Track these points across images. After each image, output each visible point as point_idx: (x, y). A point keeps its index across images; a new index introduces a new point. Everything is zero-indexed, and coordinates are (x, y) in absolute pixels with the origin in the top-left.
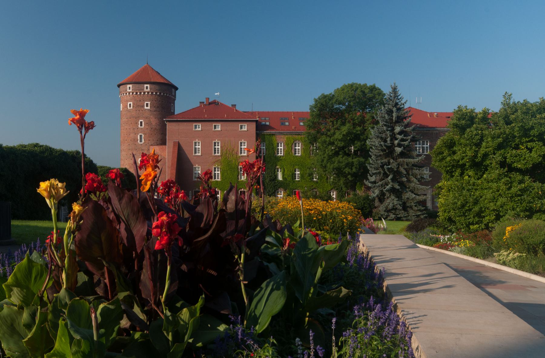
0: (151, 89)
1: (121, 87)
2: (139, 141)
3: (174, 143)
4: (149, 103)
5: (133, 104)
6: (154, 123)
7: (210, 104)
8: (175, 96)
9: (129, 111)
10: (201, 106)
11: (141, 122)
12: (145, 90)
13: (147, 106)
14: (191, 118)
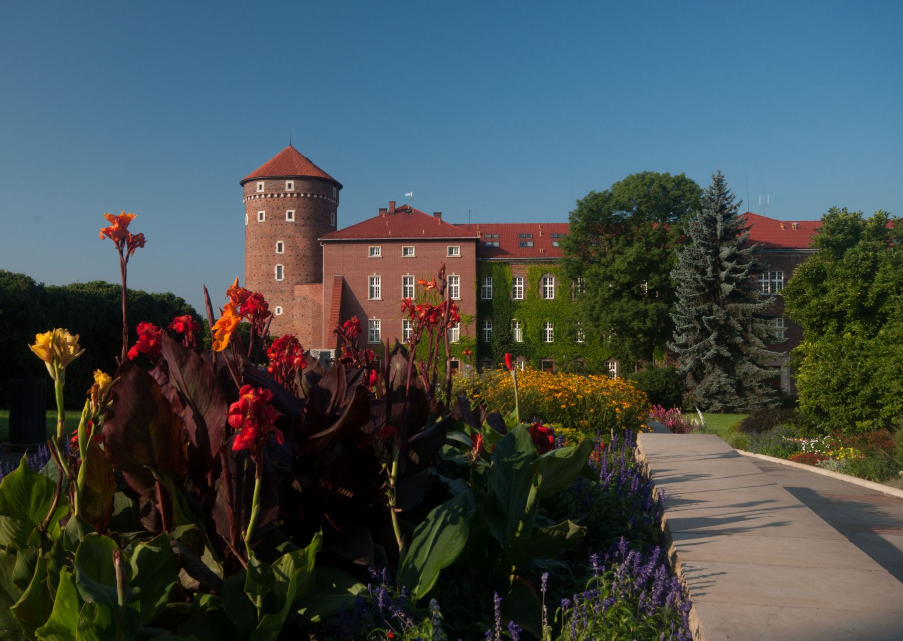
0: (296, 188)
1: (247, 185)
2: (276, 277)
3: (336, 279)
4: (293, 211)
5: (267, 213)
6: (301, 246)
7: (397, 211)
8: (337, 199)
9: (260, 226)
10: (381, 216)
11: (280, 245)
12: (287, 189)
13: (290, 217)
14: (365, 235)
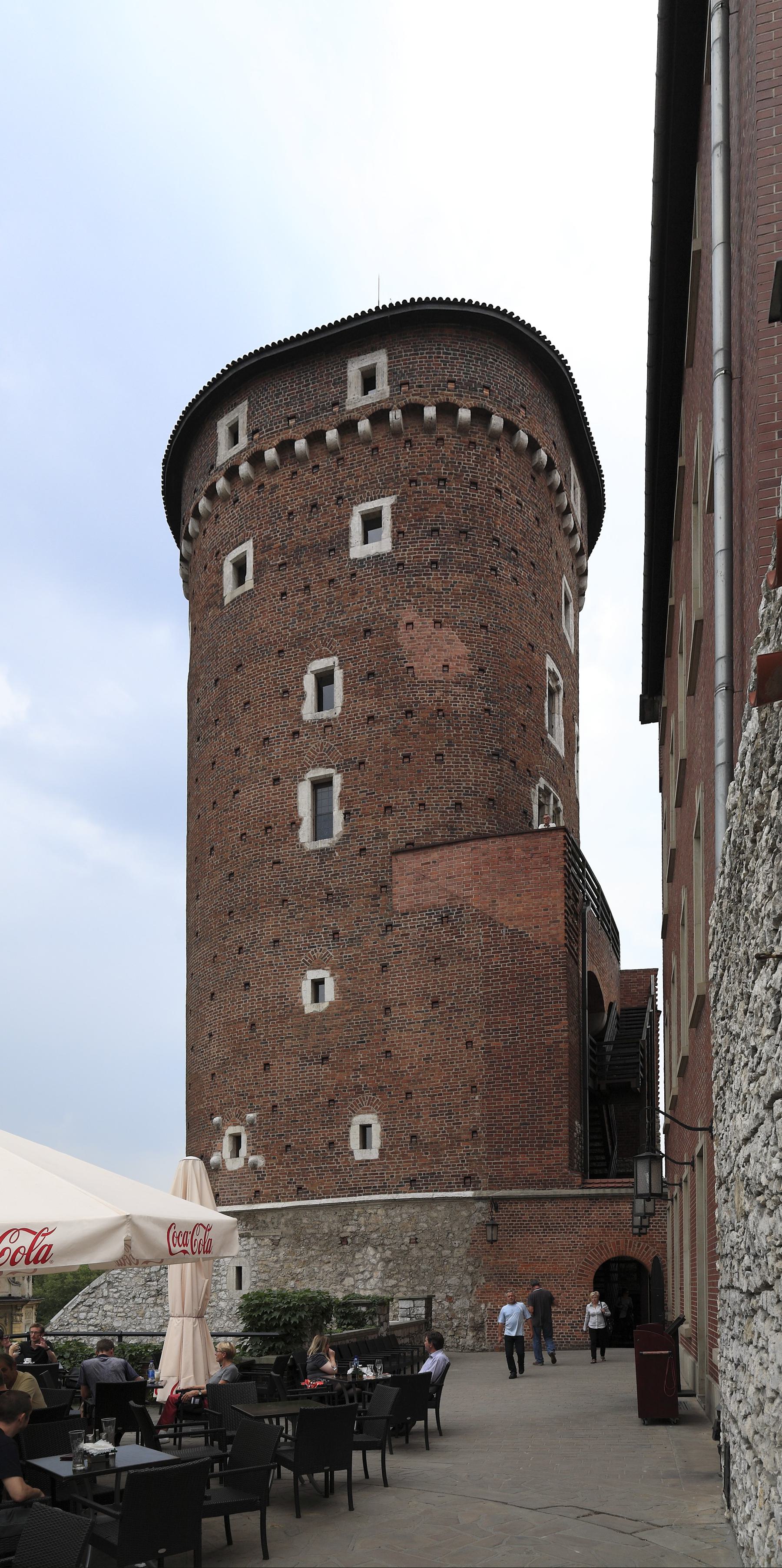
2: (305, 833)
4: (386, 504)
